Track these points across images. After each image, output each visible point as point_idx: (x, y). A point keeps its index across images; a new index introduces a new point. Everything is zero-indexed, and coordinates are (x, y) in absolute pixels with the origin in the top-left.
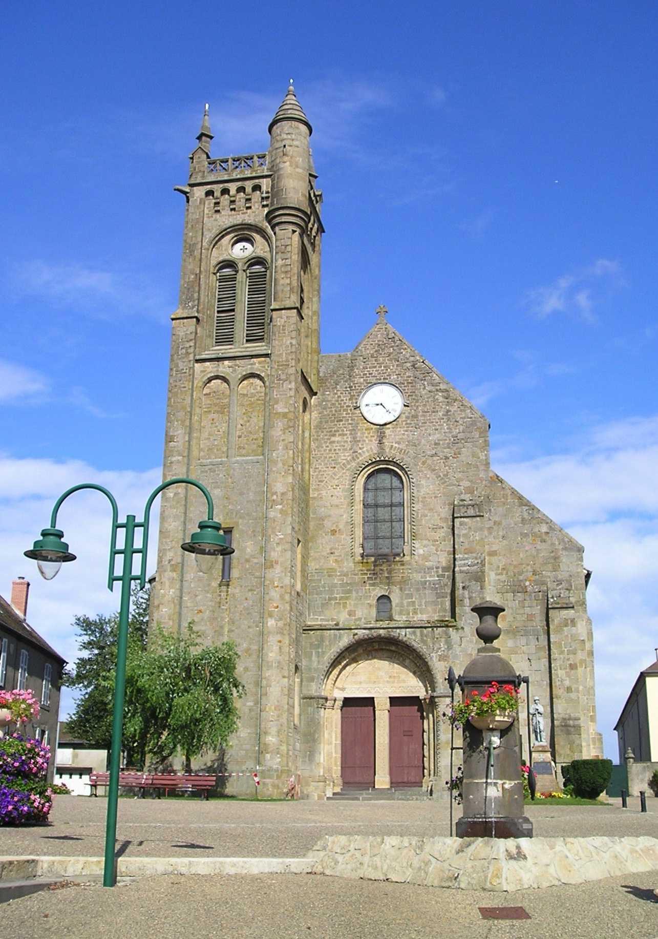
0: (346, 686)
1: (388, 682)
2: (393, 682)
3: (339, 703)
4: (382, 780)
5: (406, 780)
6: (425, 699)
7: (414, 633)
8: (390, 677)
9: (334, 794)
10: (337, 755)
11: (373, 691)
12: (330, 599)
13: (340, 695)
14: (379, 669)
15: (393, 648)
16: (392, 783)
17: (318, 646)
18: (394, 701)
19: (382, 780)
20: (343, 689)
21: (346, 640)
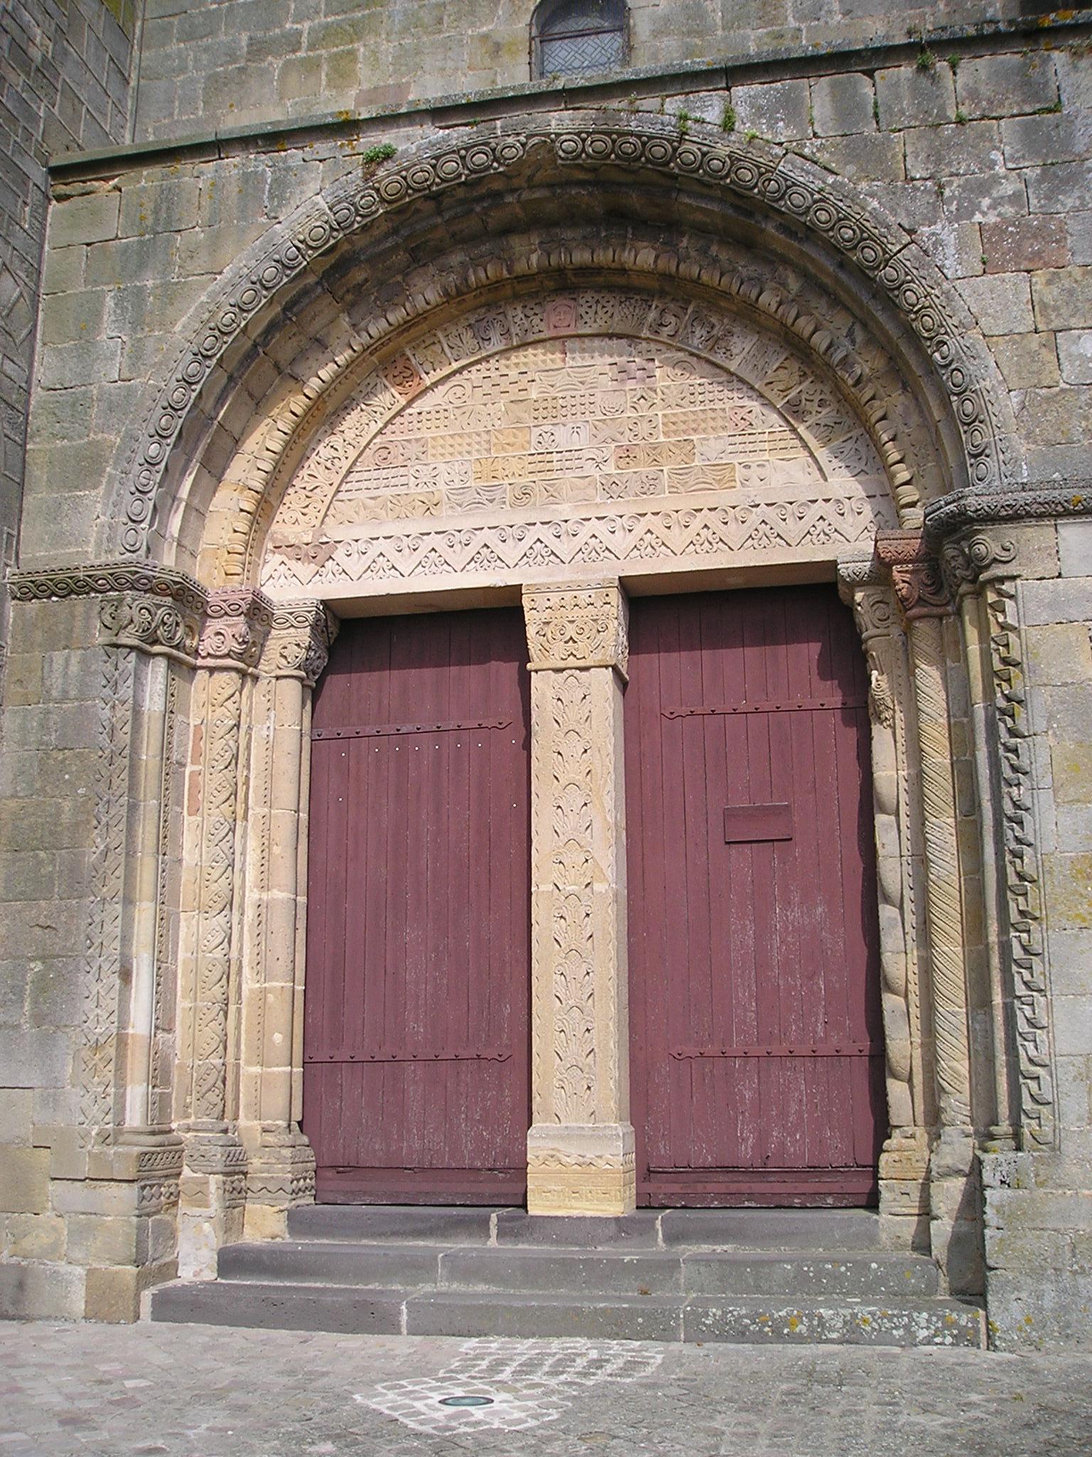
0: (334, 532)
1: (611, 488)
2: (649, 487)
3: (289, 644)
4: (579, 1155)
5: (746, 1152)
6: (882, 569)
7: (793, 108)
8: (627, 455)
9: (230, 1262)
10: (271, 985)
11: (511, 552)
12: (258, 49)
13: (294, 589)
14: (550, 411)
15: (643, 257)
16: (646, 1172)
17: (141, 258)
18: (662, 611)
19: (579, 1155)
20: (318, 553)
21: (315, 197)
